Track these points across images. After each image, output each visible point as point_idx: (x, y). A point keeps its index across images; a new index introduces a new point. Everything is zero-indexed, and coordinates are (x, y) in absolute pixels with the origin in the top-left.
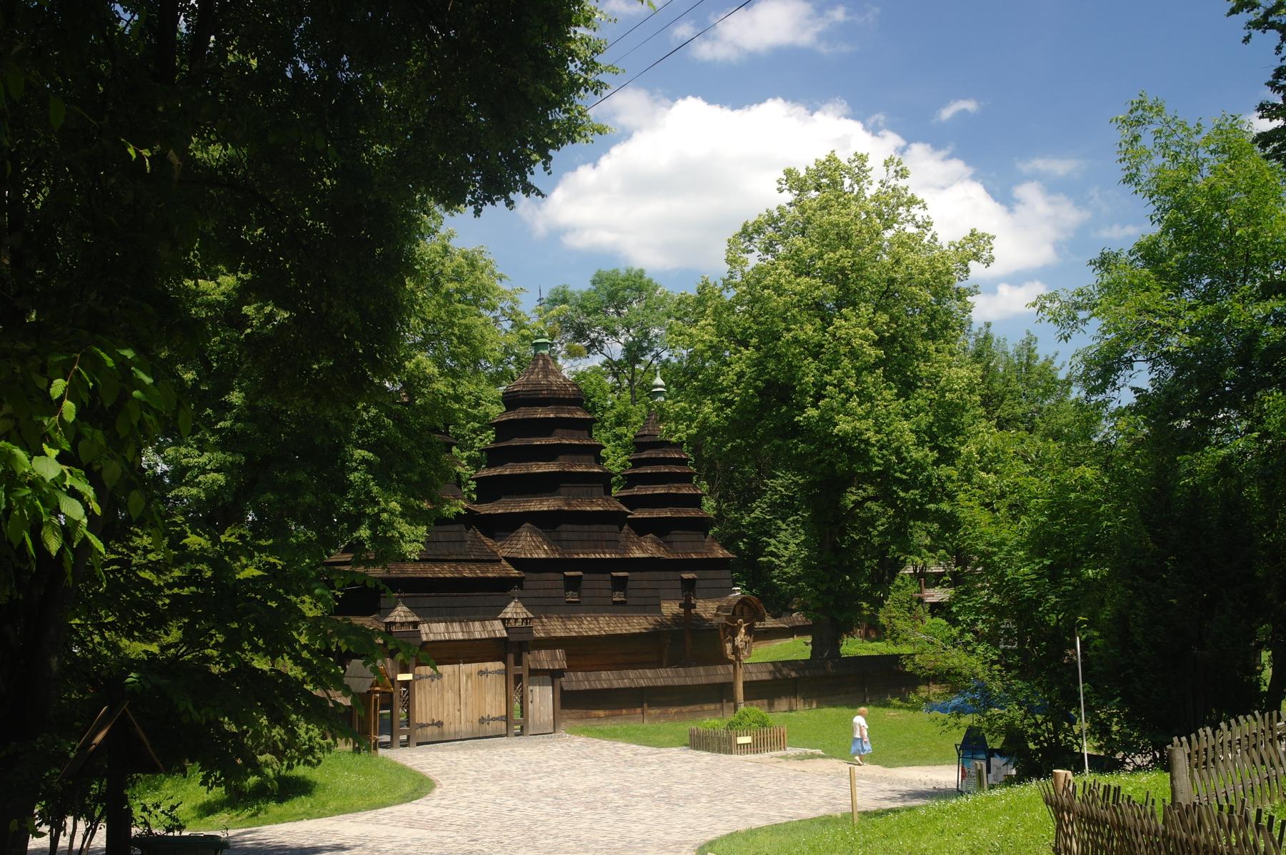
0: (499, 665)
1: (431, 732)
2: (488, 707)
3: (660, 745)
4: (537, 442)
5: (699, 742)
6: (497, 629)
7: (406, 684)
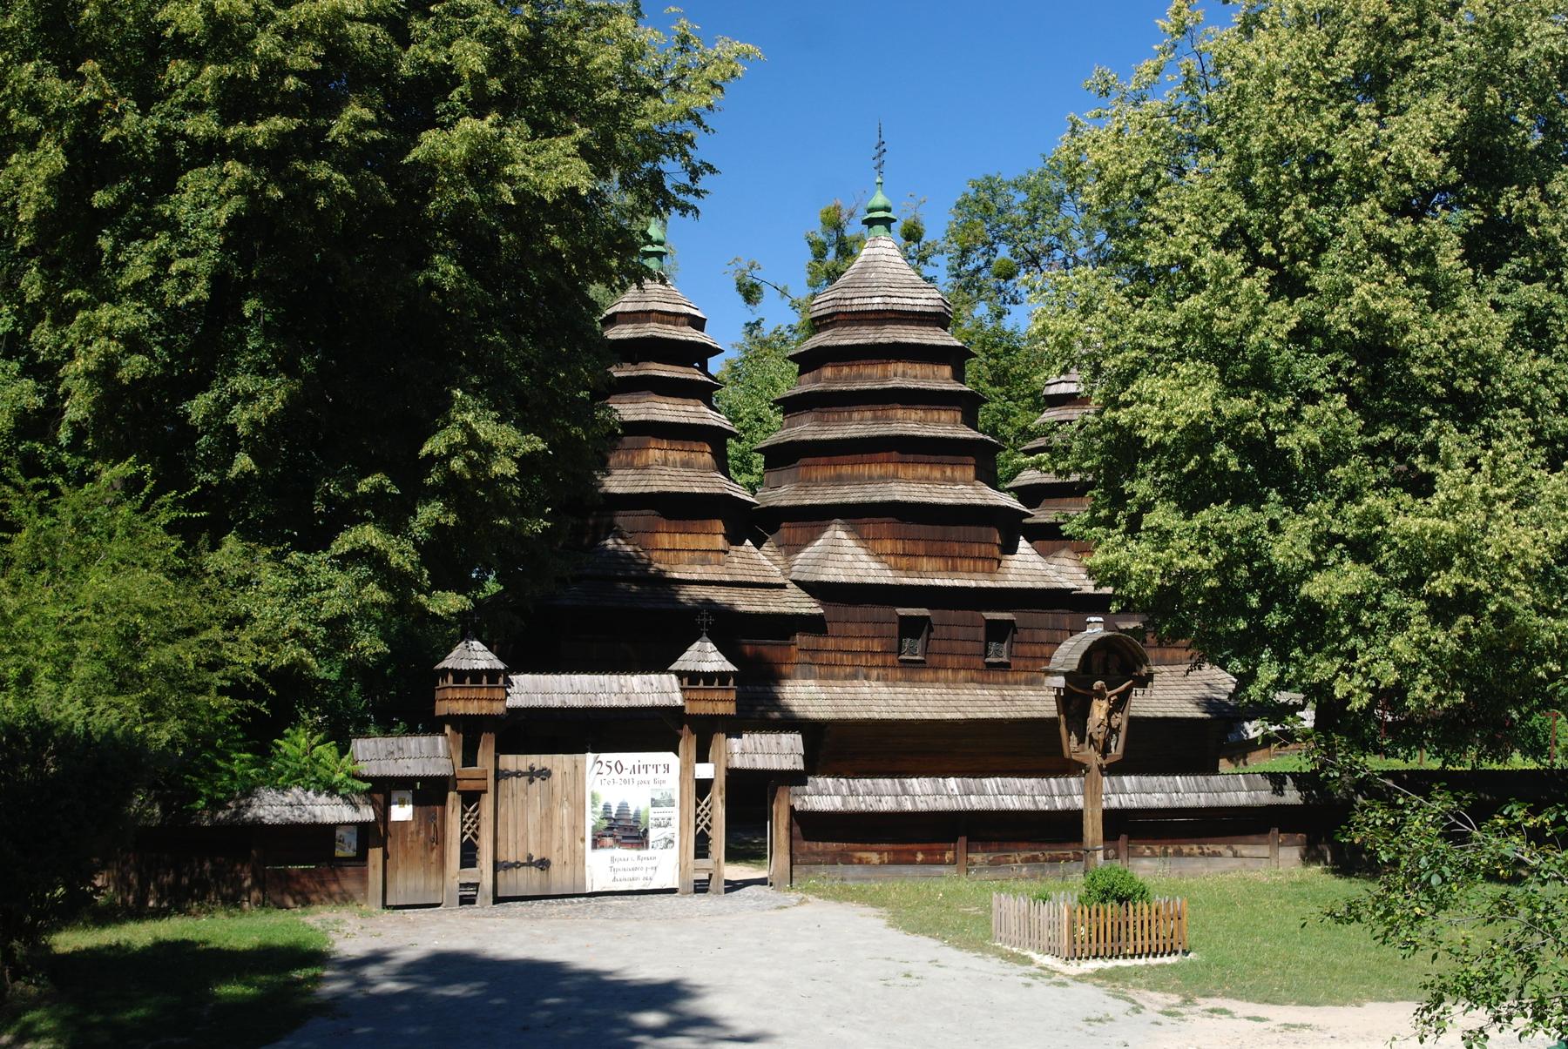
1: (526, 880)
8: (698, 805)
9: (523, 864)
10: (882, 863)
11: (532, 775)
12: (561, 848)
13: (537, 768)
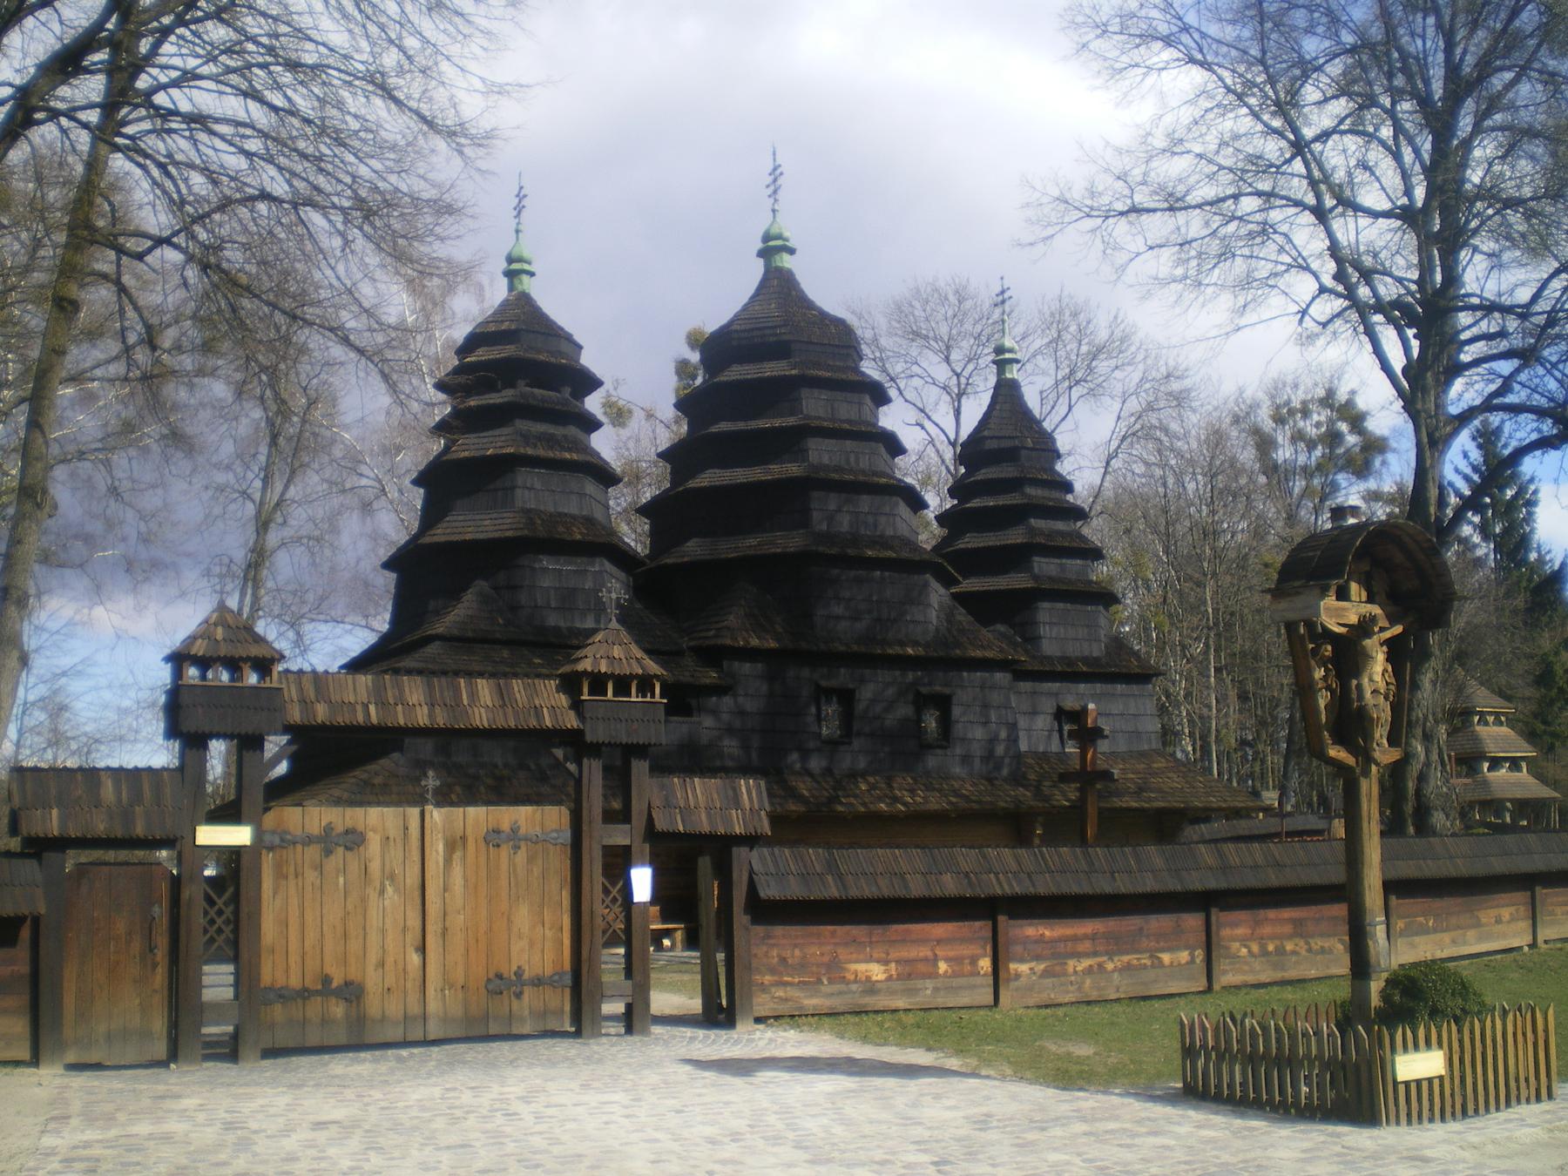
0: (550, 819)
2: (518, 946)
3: (1068, 1077)
4: (764, 424)
5: (1239, 1073)
6: (547, 703)
7: (232, 855)
8: (606, 891)
9: (318, 993)
10: (890, 978)
11: (328, 841)
12: (381, 964)
13: (340, 829)
